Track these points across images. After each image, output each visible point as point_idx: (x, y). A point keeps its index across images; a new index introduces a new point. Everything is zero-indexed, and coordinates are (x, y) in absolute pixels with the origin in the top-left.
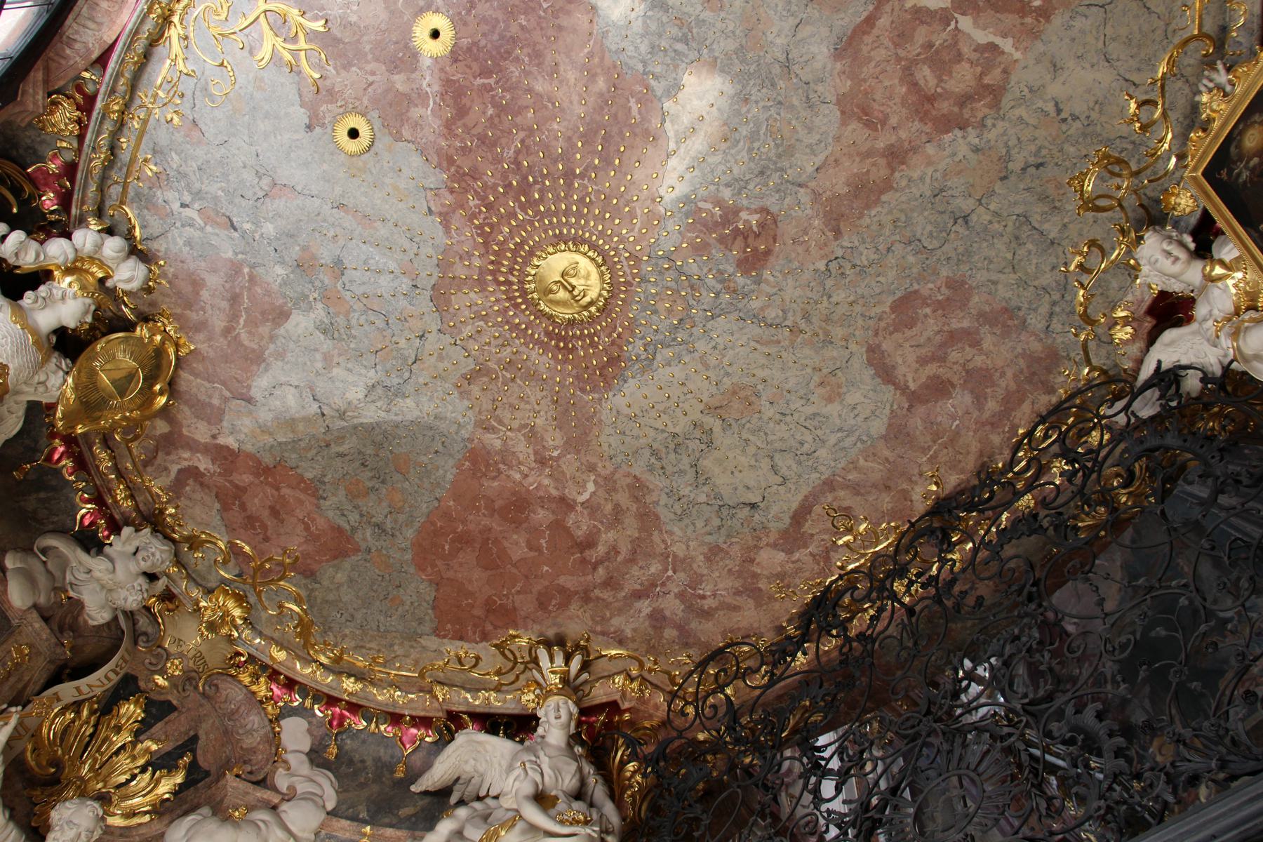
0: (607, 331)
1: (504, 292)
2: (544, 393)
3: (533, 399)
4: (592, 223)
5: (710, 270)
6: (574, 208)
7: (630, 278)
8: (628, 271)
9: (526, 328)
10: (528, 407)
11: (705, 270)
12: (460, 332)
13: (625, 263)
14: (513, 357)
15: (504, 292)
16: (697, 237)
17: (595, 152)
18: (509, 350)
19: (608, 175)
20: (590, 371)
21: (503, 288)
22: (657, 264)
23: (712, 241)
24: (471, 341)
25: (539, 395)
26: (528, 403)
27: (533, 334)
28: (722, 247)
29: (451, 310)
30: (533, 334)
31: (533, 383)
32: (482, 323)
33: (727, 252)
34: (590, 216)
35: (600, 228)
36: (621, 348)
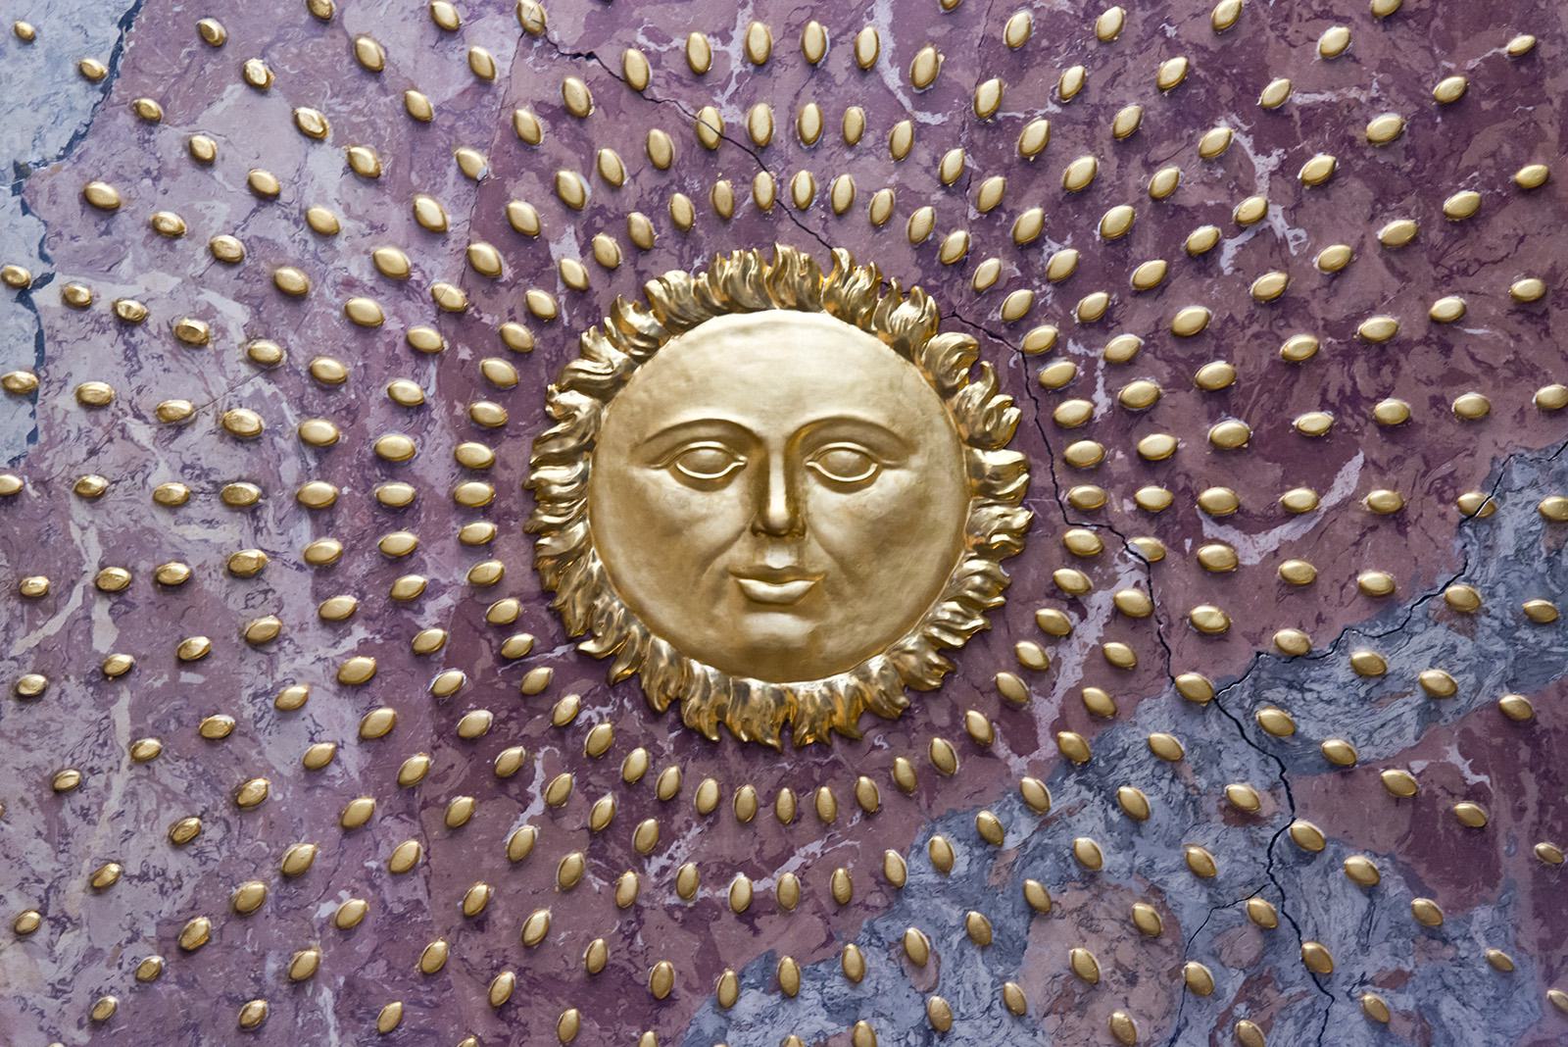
0: (727, 843)
1: (477, 277)
2: (176, 863)
3: (98, 838)
4: (1122, 344)
5: (1396, 981)
6: (1117, 216)
7: (1045, 710)
8: (1069, 675)
9: (399, 515)
10: (41, 858)
11: (1378, 961)
12: (105, 265)
13: (1090, 631)
14: (214, 585)
15: (477, 277)
16: (1475, 794)
17: (1410, 89)
18: (230, 531)
19: (1375, 218)
20: (474, 949)
21: (486, 253)
22: (1212, 755)
23: (1514, 867)
24: (108, 343)
25: (149, 848)
26: (59, 838)
27: (399, 563)
28: (1531, 932)
29: (168, 139)
30: (399, 563)
31: (173, 776)
32: (235, 315)
33: (1530, 973)
34: (1144, 313)
35: (1139, 389)
36: (709, 965)
